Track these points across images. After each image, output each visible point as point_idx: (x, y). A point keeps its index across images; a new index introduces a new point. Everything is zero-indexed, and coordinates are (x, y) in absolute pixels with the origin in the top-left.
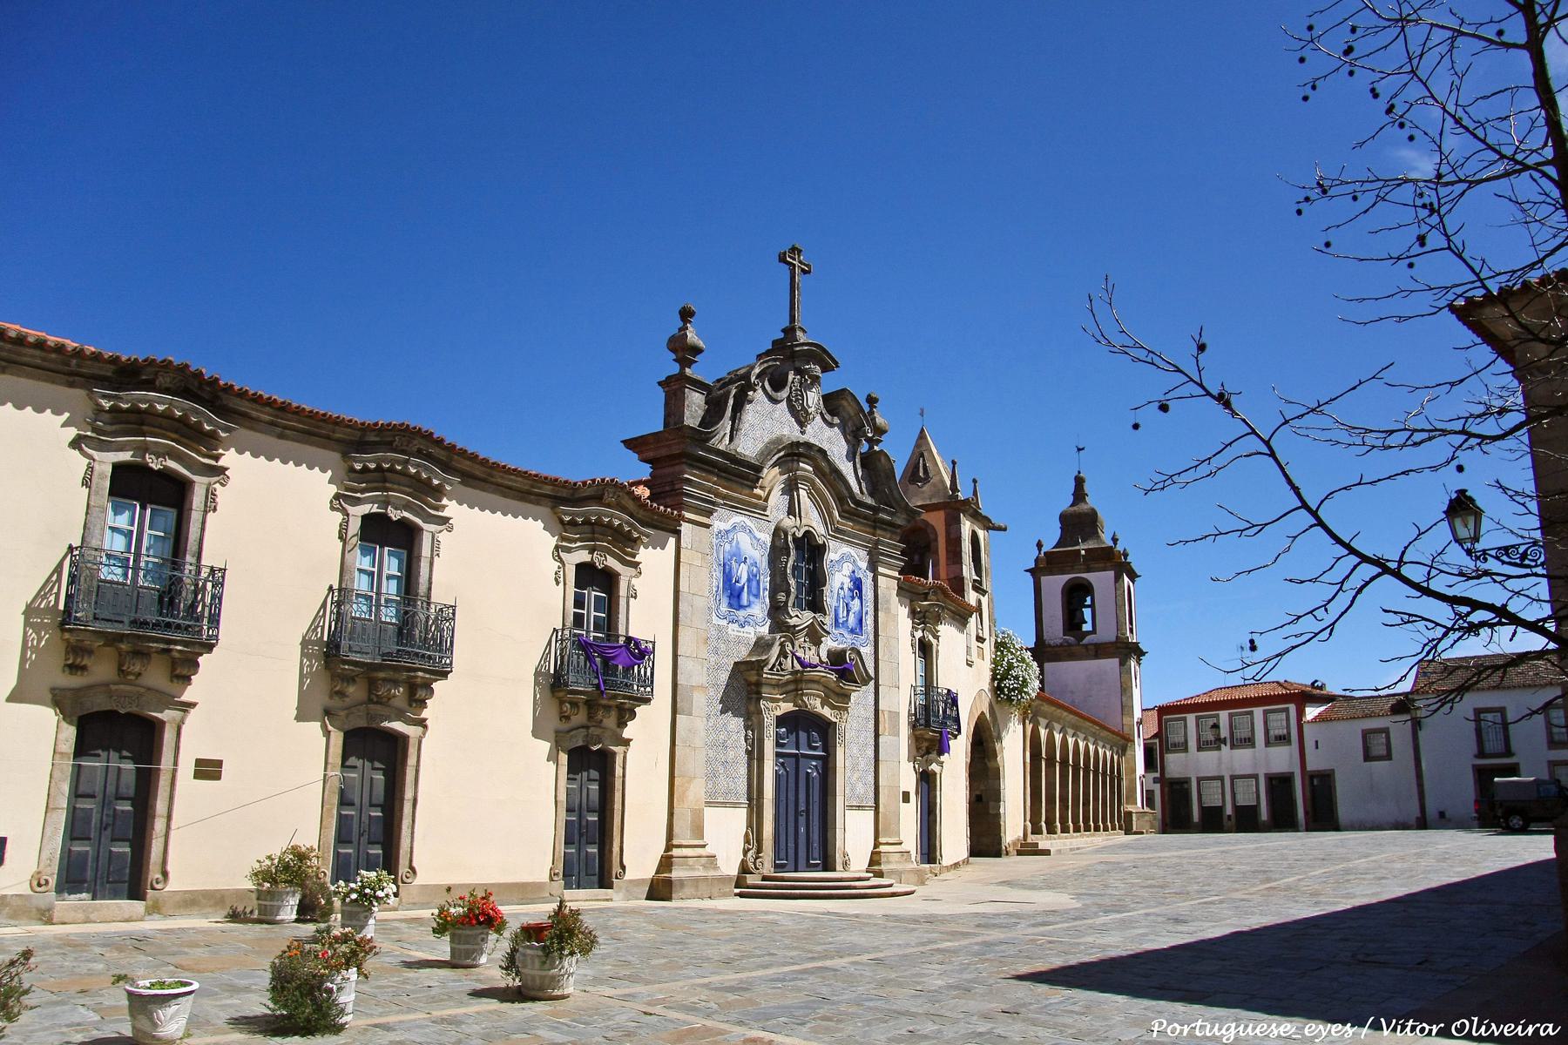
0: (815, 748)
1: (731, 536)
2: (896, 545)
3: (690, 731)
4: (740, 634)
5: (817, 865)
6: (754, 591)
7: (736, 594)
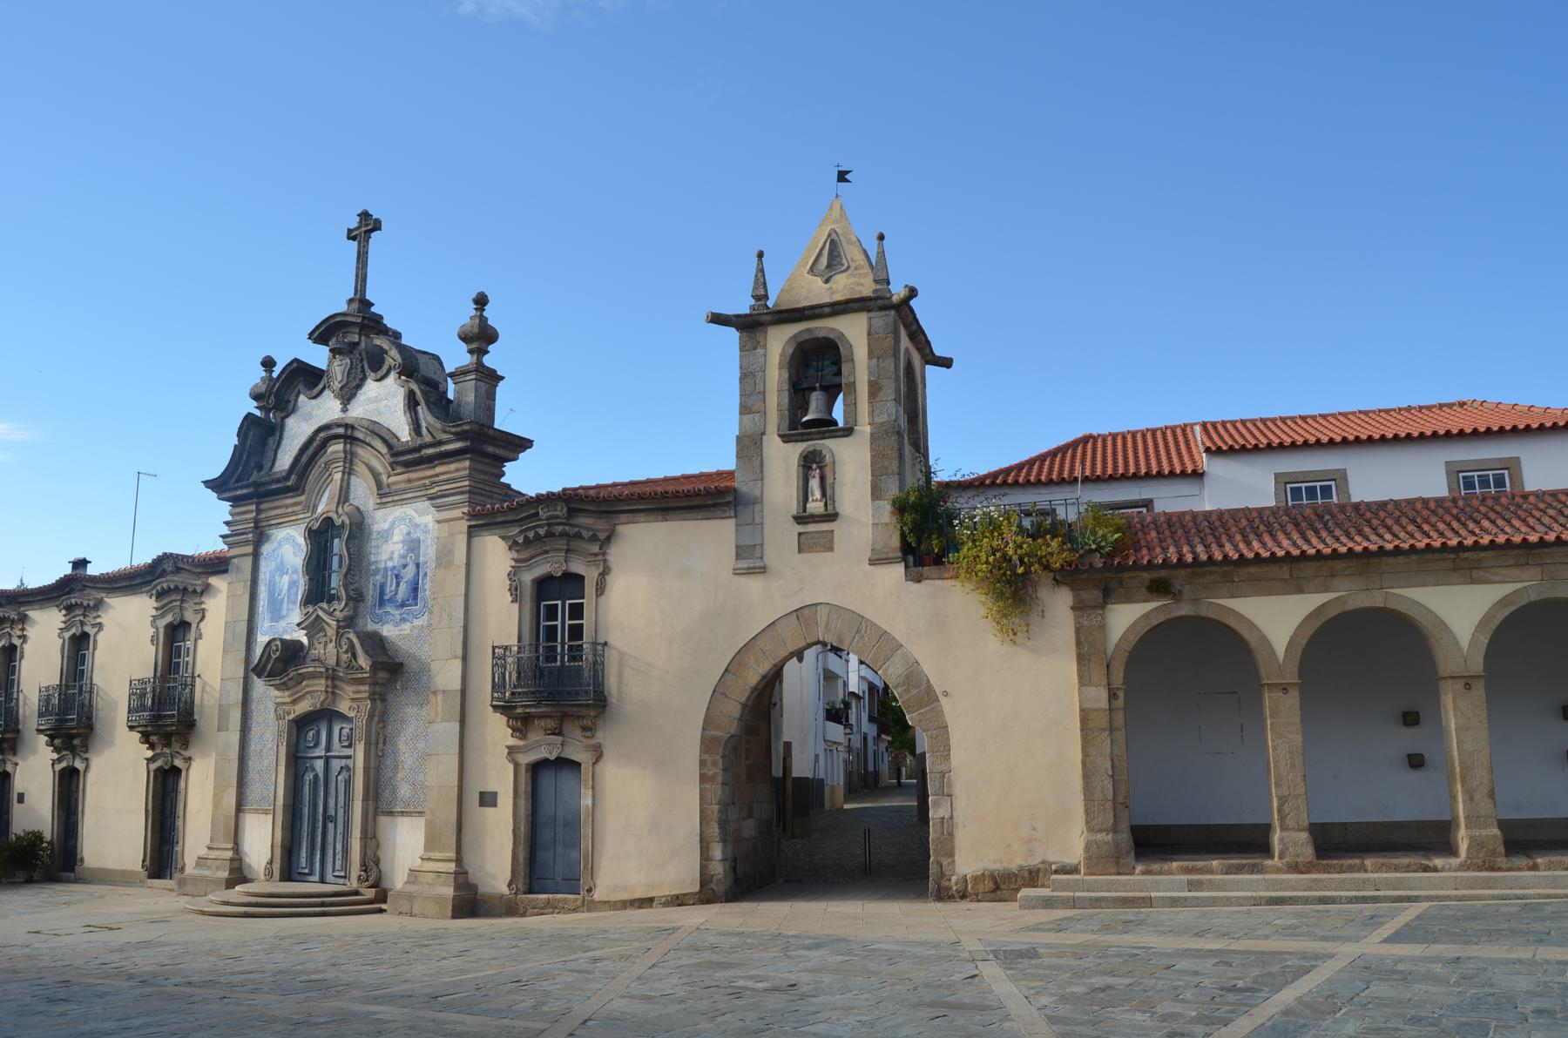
1: (276, 554)
6: (293, 598)
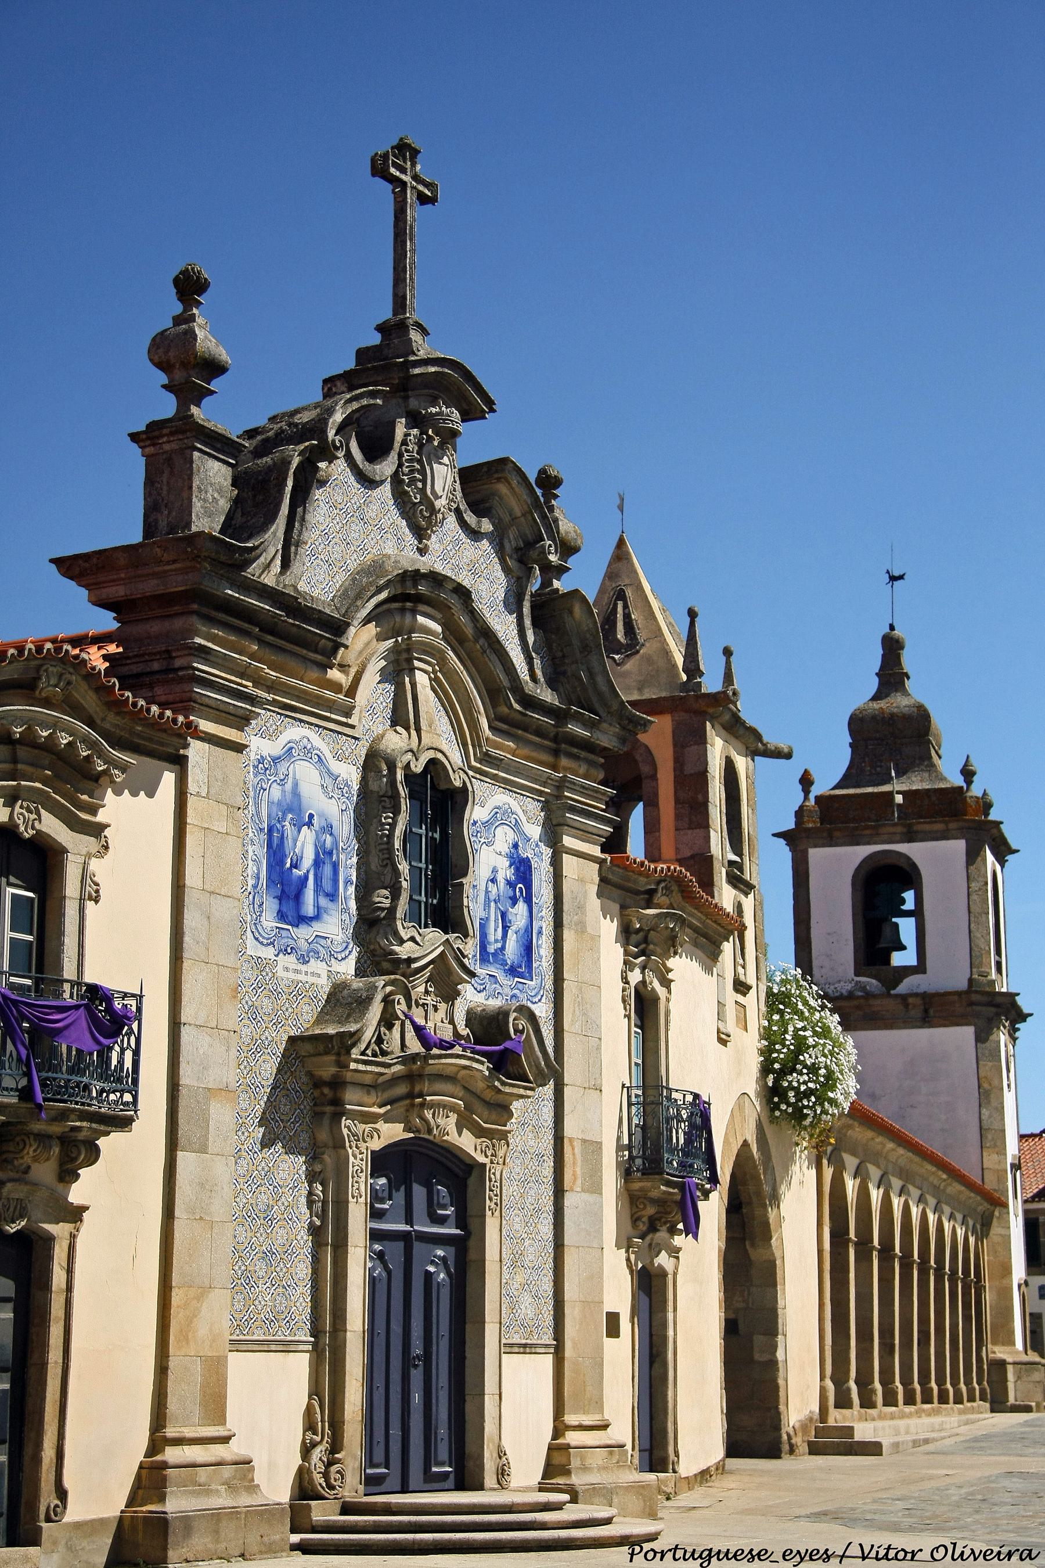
0: (442, 1221)
1: (282, 768)
2: (597, 791)
3: (202, 1185)
4: (300, 977)
5: (446, 1475)
6: (327, 885)
7: (292, 891)
